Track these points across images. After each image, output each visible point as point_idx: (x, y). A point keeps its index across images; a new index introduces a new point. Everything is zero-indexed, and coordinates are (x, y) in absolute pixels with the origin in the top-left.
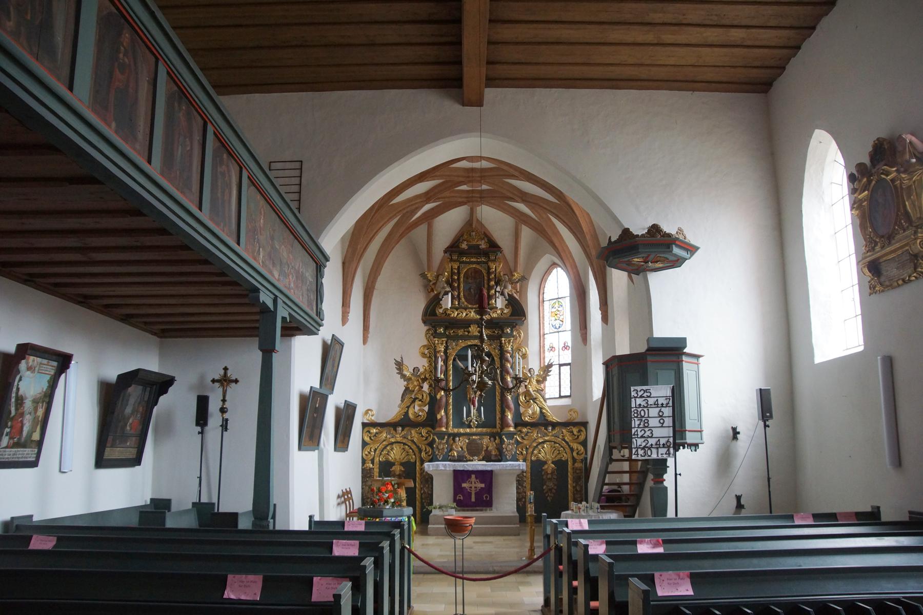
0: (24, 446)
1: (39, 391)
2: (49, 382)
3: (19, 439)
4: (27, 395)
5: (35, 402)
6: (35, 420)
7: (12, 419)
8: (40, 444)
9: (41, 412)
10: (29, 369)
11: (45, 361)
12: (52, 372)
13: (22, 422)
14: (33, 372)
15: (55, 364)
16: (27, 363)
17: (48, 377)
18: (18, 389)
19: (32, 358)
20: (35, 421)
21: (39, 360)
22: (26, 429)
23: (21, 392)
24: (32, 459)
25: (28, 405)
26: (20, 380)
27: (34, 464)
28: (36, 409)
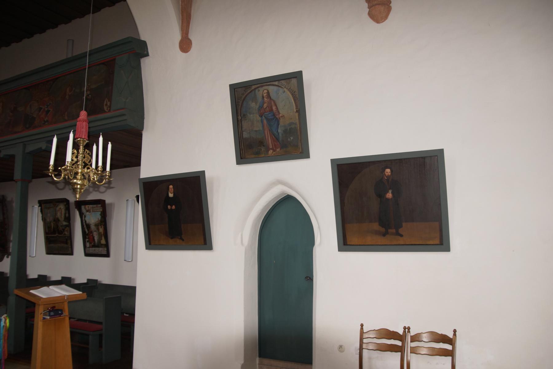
0: (98, 246)
1: (97, 220)
2: (101, 215)
3: (94, 243)
4: (91, 223)
5: (97, 225)
6: (100, 234)
7: (87, 234)
8: (107, 246)
9: (101, 230)
10: (87, 211)
11: (95, 206)
12: (101, 210)
13: (92, 235)
14: (90, 212)
15: (100, 205)
16: (85, 209)
17: (100, 213)
18: (86, 221)
19: (87, 206)
20: (100, 235)
21: (91, 206)
22: (96, 239)
23: (87, 222)
24: (105, 253)
25: (93, 227)
26: (85, 217)
27: (107, 255)
28: (98, 229)
